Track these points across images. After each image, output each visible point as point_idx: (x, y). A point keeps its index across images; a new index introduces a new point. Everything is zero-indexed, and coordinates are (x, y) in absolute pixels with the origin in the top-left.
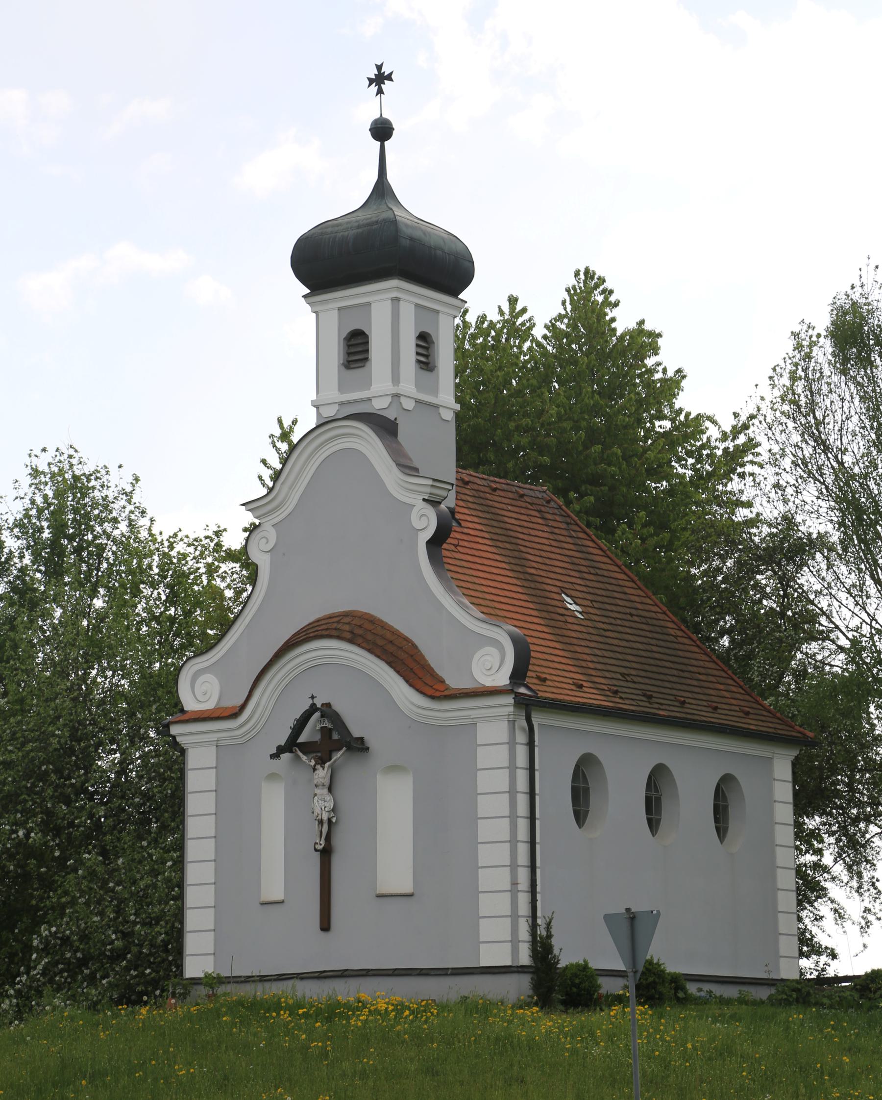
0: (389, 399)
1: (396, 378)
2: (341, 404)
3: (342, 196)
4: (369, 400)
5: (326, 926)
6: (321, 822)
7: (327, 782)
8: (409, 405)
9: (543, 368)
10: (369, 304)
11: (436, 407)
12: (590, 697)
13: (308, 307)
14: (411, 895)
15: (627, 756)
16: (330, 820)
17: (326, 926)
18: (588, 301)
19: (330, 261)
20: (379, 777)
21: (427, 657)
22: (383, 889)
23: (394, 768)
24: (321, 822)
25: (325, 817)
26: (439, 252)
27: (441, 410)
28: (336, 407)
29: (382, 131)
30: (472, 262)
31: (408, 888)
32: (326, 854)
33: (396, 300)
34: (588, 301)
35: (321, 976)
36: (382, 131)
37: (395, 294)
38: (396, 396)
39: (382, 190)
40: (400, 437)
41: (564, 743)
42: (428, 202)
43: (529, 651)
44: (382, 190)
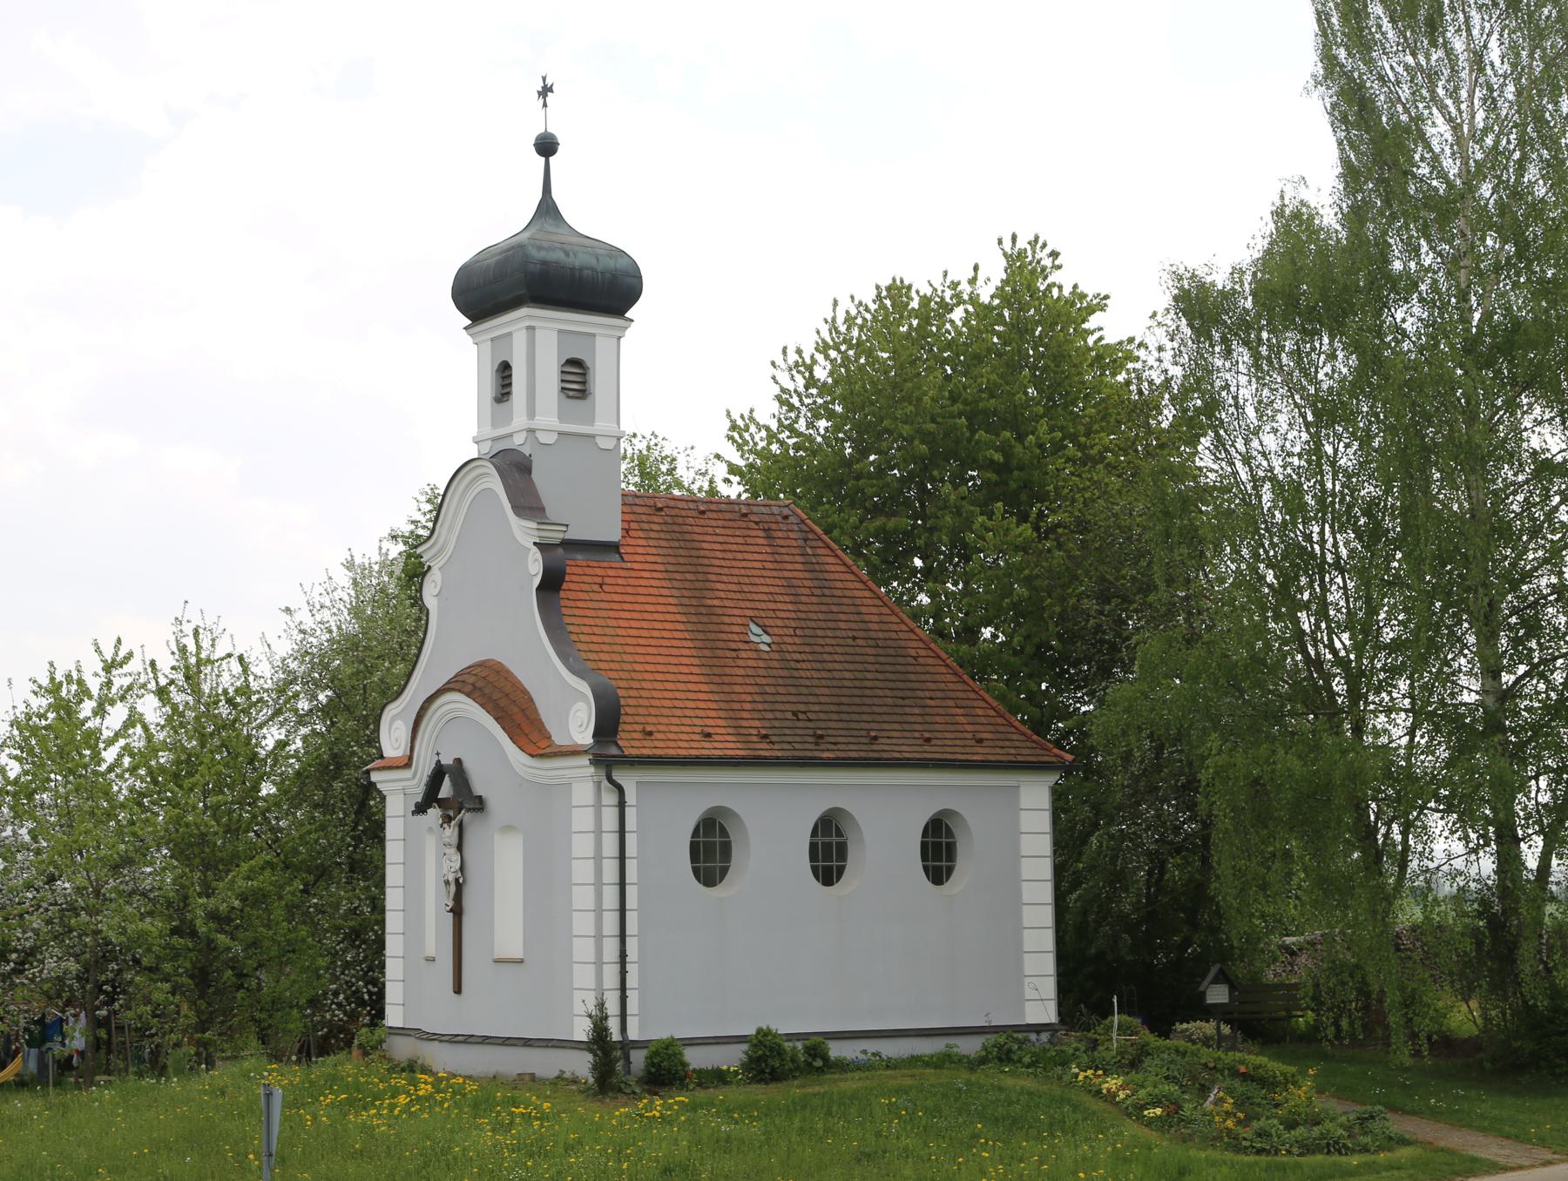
0: (524, 434)
1: (531, 413)
2: (494, 440)
3: (501, 220)
4: (511, 435)
5: (458, 990)
6: (447, 883)
7: (455, 841)
8: (545, 438)
9: (971, 352)
10: (510, 334)
11: (593, 436)
12: (734, 749)
13: (470, 339)
14: (521, 961)
15: (774, 814)
16: (457, 880)
17: (458, 990)
18: (1024, 272)
19: (485, 293)
20: (498, 838)
21: (541, 711)
22: (501, 953)
23: (508, 828)
24: (447, 883)
25: (451, 878)
26: (586, 272)
27: (598, 440)
28: (489, 443)
29: (546, 146)
30: (640, 277)
31: (519, 955)
32: (457, 911)
33: (531, 329)
34: (1024, 272)
35: (454, 1039)
36: (546, 146)
37: (527, 323)
38: (531, 431)
39: (547, 208)
40: (534, 476)
41: (668, 808)
42: (597, 216)
43: (619, 707)
44: (547, 208)
